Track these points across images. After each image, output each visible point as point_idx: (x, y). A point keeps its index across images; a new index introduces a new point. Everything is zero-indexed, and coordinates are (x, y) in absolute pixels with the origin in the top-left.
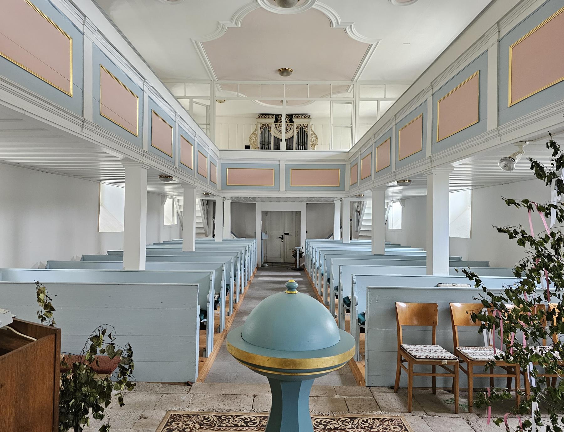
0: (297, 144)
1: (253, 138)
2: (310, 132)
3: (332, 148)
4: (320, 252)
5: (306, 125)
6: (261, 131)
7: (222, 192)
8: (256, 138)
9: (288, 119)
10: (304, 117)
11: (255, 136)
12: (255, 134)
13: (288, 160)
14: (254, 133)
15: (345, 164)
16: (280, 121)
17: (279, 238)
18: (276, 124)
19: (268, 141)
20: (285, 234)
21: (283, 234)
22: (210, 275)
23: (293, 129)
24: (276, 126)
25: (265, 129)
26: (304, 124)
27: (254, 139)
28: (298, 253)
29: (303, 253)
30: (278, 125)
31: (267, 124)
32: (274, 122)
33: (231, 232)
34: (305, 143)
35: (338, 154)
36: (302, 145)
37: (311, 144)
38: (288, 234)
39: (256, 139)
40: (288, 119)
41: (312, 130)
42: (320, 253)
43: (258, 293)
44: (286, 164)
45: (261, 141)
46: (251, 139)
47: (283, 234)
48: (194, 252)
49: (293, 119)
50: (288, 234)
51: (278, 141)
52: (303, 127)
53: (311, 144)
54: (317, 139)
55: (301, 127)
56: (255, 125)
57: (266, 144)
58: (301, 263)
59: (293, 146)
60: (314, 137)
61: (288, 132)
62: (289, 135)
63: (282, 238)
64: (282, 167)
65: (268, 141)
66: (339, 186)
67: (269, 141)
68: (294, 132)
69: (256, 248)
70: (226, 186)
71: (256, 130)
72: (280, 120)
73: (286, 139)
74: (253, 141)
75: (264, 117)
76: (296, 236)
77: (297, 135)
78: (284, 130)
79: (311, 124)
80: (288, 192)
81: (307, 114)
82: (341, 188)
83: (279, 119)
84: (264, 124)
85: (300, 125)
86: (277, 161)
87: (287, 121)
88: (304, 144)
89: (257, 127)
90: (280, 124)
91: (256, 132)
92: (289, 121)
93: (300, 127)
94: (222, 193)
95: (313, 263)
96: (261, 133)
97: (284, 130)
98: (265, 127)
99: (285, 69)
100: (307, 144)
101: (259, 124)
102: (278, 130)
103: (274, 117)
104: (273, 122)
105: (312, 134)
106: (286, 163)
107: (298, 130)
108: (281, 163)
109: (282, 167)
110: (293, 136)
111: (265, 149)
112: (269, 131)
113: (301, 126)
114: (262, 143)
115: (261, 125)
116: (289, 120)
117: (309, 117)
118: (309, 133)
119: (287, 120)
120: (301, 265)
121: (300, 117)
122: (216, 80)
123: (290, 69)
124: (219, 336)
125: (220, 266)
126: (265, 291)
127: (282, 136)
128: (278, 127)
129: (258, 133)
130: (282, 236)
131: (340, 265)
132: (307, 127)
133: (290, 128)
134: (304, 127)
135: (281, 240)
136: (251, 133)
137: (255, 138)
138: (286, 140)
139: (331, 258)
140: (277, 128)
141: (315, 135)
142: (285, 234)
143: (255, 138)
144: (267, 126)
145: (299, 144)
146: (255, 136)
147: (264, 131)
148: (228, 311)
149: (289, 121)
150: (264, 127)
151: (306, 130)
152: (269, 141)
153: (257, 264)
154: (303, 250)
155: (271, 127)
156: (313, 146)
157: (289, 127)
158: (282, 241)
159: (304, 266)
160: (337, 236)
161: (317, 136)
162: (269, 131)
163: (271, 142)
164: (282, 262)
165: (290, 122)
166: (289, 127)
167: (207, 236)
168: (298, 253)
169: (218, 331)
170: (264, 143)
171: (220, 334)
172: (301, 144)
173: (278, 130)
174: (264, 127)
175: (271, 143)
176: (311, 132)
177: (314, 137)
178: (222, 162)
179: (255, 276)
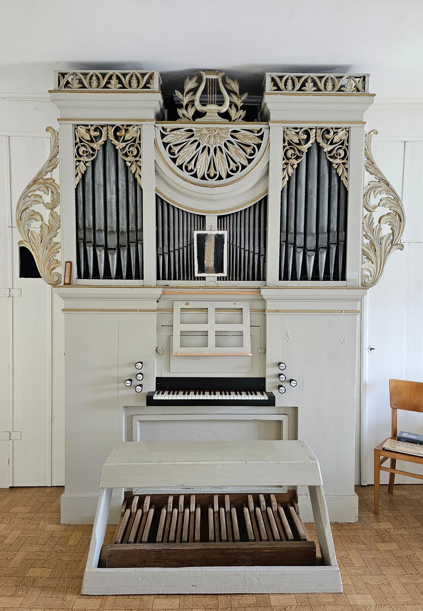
1: (37, 208)
5: (341, 134)
6: (82, 168)
8: (57, 210)
9: (235, 99)
11: (48, 199)
16: (191, 112)
18: (170, 126)
19: (123, 227)
24: (169, 138)
26: (328, 132)
27: (46, 213)
31: (117, 129)
32: (160, 118)
34: (333, 238)
36: (317, 250)
37: (368, 241)
52: (320, 148)
55: (309, 145)
56: (49, 134)
57: (112, 242)
61: (236, 175)
65: (123, 227)
67: (132, 226)
72: (192, 103)
79: (367, 129)
83: (185, 100)
85: (307, 132)
87: (233, 113)
88: (323, 240)
92: (242, 113)
93: (304, 148)
96: (84, 176)
98: (104, 146)
101: (69, 129)
102: (179, 162)
104: (152, 116)
107: (296, 162)
110: (266, 198)
112: (126, 168)
113: (312, 140)
114: (90, 236)
115: (82, 131)
116: (240, 104)
119: (231, 104)
121: (309, 85)
128: (181, 145)
134: (327, 148)
137: (46, 205)
140: (176, 150)
143: (52, 207)
144: (117, 138)
145: (300, 242)
149: (242, 113)
150: (97, 146)
151: (338, 161)
152: (132, 226)
157: (243, 146)
163: (139, 231)
165: (248, 119)
166: (243, 146)
170: (101, 238)
172: (311, 243)
173: (179, 162)
174: (97, 146)
175: (139, 241)
176: (368, 178)
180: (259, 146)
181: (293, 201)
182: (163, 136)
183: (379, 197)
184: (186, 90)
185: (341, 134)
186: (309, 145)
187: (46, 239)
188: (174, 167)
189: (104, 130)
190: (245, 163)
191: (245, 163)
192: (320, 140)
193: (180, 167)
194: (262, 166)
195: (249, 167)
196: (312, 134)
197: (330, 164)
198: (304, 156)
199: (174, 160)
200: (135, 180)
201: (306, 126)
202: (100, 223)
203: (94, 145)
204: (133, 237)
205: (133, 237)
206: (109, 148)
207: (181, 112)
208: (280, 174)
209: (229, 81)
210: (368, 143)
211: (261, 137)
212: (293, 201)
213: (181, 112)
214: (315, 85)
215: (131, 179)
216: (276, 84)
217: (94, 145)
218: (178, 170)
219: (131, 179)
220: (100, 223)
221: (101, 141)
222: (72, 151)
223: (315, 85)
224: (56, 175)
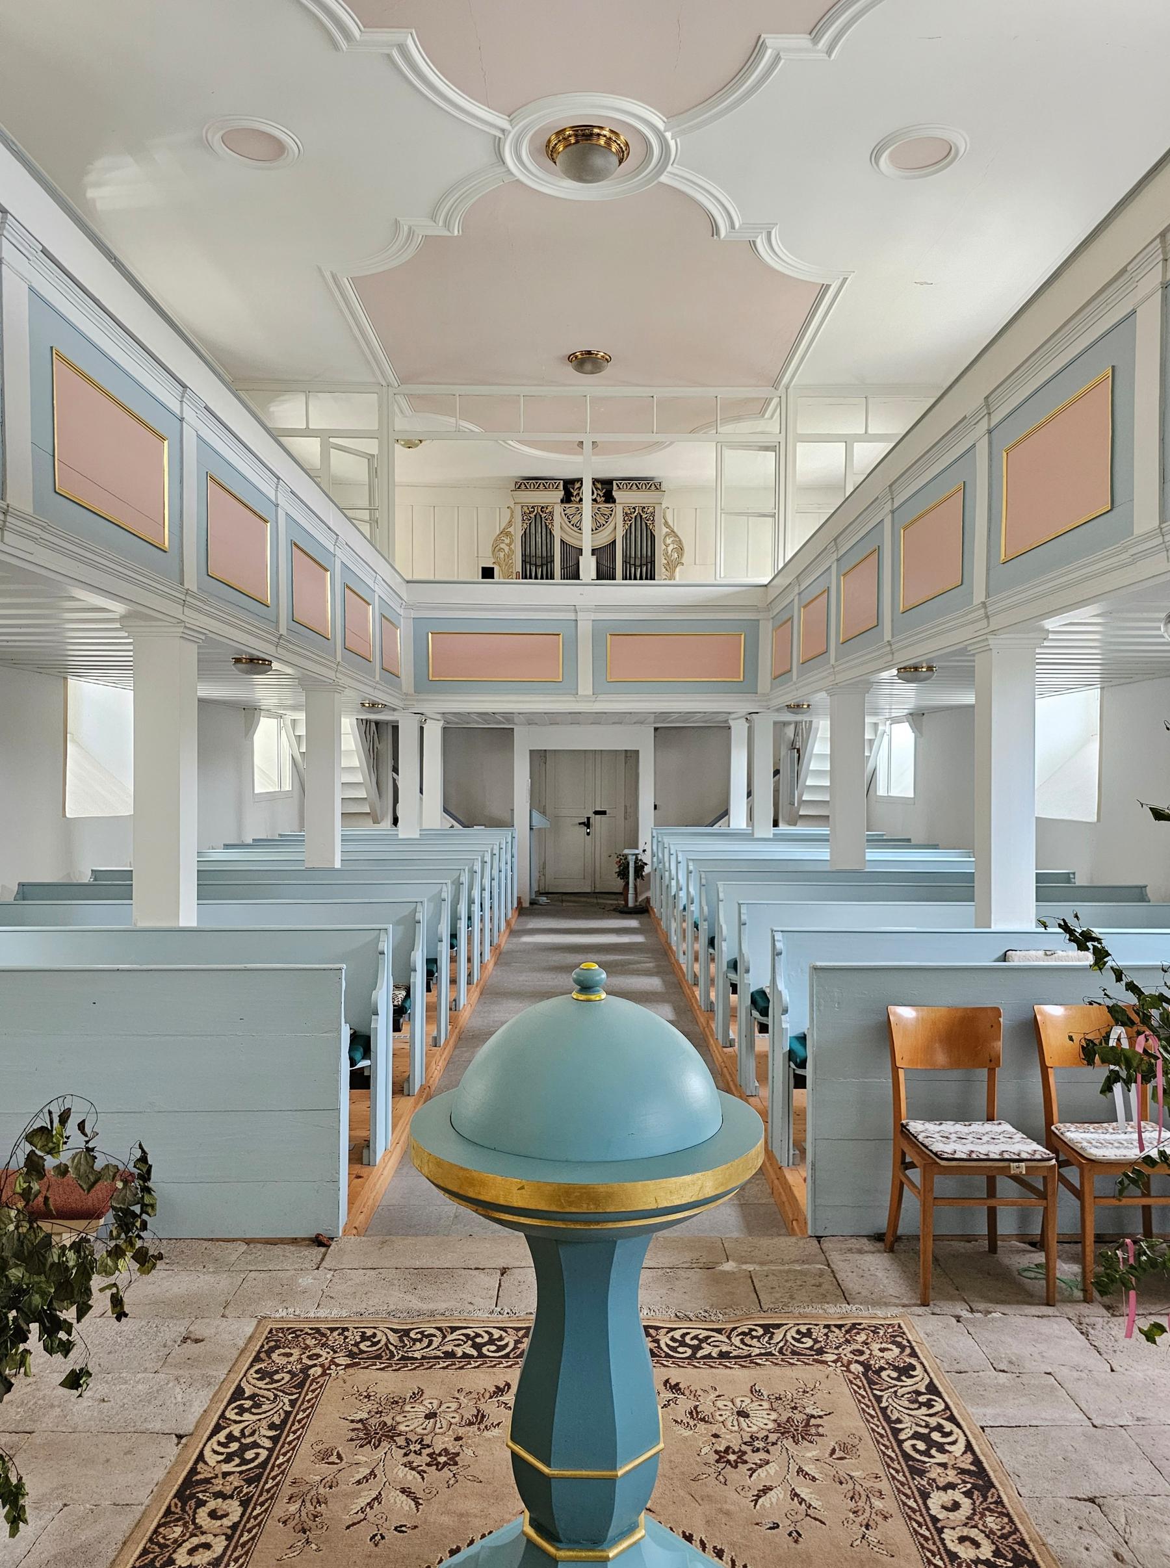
0: (625, 562)
1: (502, 546)
2: (661, 530)
3: (722, 576)
4: (691, 863)
5: (651, 509)
7: (418, 700)
8: (512, 546)
9: (599, 492)
10: (644, 486)
11: (507, 541)
12: (508, 534)
13: (599, 608)
14: (505, 533)
15: (758, 620)
16: (578, 499)
17: (580, 824)
18: (567, 506)
19: (545, 554)
20: (596, 813)
21: (591, 815)
22: (378, 937)
23: (613, 523)
25: (537, 519)
26: (644, 508)
27: (507, 549)
28: (632, 865)
29: (646, 864)
30: (573, 511)
31: (543, 507)
32: (562, 501)
33: (446, 810)
34: (649, 560)
35: (738, 592)
36: (641, 566)
37: (666, 562)
38: (604, 813)
39: (510, 549)
40: (599, 492)
41: (666, 524)
42: (691, 868)
43: (521, 979)
44: (593, 620)
45: (524, 555)
46: (496, 549)
47: (591, 815)
48: (337, 870)
49: (614, 493)
50: (604, 813)
51: (574, 553)
52: (641, 516)
53: (666, 562)
54: (680, 549)
55: (635, 514)
57: (539, 563)
58: (643, 892)
59: (614, 569)
60: (673, 542)
62: (603, 539)
63: (587, 824)
64: (585, 629)
65: (545, 554)
66: (742, 679)
67: (549, 554)
68: (616, 529)
69: (516, 855)
70: (426, 684)
71: (510, 524)
72: (578, 494)
73: (593, 550)
74: (502, 554)
75: (532, 486)
76: (625, 819)
77: (626, 537)
78: (587, 523)
79: (664, 506)
80: (601, 697)
81: (652, 479)
82: (748, 686)
84: (533, 507)
85: (634, 508)
86: (569, 611)
87: (598, 499)
88: (644, 562)
89: (512, 516)
90: (577, 506)
91: (511, 529)
92: (603, 499)
93: (633, 516)
94: (415, 703)
95: (673, 894)
96: (525, 532)
97: (587, 523)
98: (535, 516)
99: (589, 353)
100: (653, 562)
101: (519, 507)
102: (572, 523)
103: (561, 487)
105: (667, 535)
106: (593, 616)
108: (581, 616)
109: (585, 629)
110: (615, 540)
111: (536, 578)
112: (546, 526)
114: (528, 560)
115: (526, 508)
117: (658, 487)
118: (660, 531)
119: (598, 494)
120: (640, 900)
121: (634, 486)
122: (396, 385)
123: (602, 354)
124: (406, 1103)
125: (406, 911)
126: (539, 975)
127: (582, 540)
129: (517, 531)
130: (588, 819)
131: (741, 902)
132: (653, 514)
133: (607, 517)
135: (584, 829)
136: (498, 533)
137: (507, 545)
138: (594, 552)
139: (718, 883)
140: (571, 517)
141: (677, 536)
142: (596, 813)
143: (509, 545)
144: (542, 512)
145: (632, 562)
146: (507, 541)
147: (533, 525)
148: (435, 1034)
149: (603, 499)
152: (549, 554)
153: (519, 899)
154: (646, 858)
155: (552, 514)
156: (671, 567)
158: (588, 834)
159: (648, 900)
160: (738, 819)
161: (680, 541)
162: (546, 526)
164: (589, 891)
165: (606, 501)
167: (376, 821)
168: (632, 865)
169: (406, 1092)
171: (411, 1100)
172: (638, 563)
173: (572, 523)
176: (665, 530)
177: (673, 542)
178: (413, 614)
179: (513, 933)
180: (611, 515)
181: (628, 541)
182: (564, 510)
183: (672, 539)
184: (576, 487)
185: (651, 509)
186: (635, 514)
187: (506, 560)
188: (570, 525)
189: (536, 508)
190: (604, 523)
191: (604, 523)
192: (641, 512)
193: (573, 525)
194: (612, 525)
195: (606, 525)
196: (637, 509)
197: (646, 523)
198: (633, 520)
199: (570, 522)
200: (551, 532)
201: (634, 505)
202: (533, 553)
203: (531, 515)
204: (549, 560)
205: (549, 560)
206: (538, 516)
207: (572, 499)
208: (622, 528)
209: (596, 483)
210: (664, 513)
211: (612, 511)
212: (628, 541)
213: (572, 499)
214: (637, 486)
215: (548, 531)
216: (618, 486)
217: (531, 515)
218: (572, 527)
219: (548, 531)
220: (533, 553)
221: (534, 514)
222: (520, 518)
223: (637, 486)
224: (511, 529)
